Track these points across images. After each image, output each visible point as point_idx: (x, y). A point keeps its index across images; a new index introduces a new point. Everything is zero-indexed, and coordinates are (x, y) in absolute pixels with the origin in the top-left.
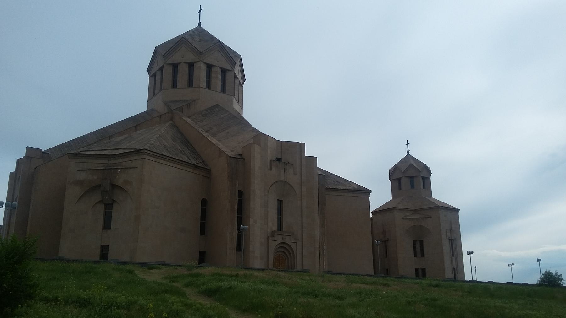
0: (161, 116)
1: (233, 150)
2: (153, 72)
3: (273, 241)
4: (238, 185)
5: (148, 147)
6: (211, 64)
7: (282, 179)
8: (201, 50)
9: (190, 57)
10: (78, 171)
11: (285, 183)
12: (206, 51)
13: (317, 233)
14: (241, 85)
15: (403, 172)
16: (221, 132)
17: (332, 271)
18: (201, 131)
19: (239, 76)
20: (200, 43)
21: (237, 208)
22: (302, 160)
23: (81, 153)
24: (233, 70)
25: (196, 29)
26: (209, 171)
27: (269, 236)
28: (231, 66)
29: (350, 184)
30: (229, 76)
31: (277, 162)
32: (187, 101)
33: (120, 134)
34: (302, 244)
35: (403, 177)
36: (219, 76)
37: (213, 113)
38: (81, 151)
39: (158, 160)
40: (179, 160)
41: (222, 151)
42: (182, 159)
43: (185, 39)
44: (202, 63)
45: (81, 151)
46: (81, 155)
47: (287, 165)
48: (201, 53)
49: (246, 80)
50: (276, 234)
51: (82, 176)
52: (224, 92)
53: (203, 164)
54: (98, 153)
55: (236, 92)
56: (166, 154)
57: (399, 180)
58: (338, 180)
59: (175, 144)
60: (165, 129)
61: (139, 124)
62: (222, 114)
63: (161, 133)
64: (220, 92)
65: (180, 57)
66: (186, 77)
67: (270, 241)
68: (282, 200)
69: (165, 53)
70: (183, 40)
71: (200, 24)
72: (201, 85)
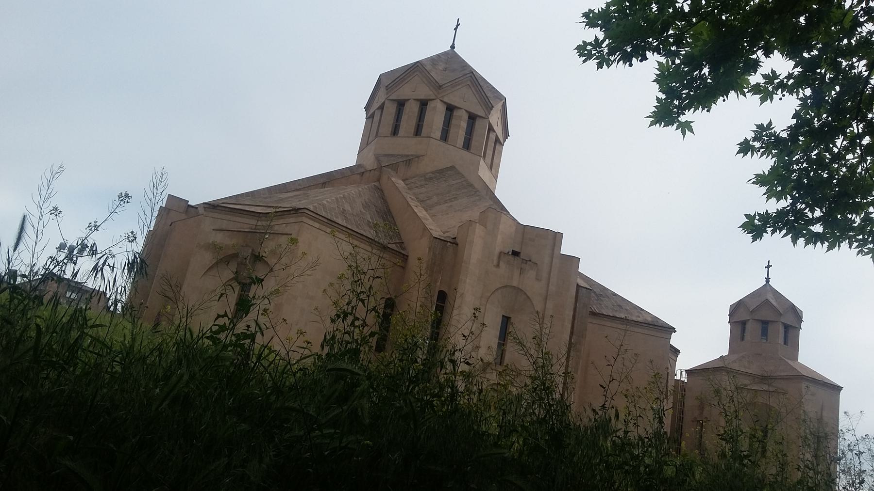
0: (363, 173)
1: (449, 230)
2: (372, 111)
4: (439, 283)
5: (313, 206)
6: (453, 104)
7: (515, 284)
8: (441, 83)
9: (424, 92)
10: (213, 230)
11: (518, 290)
12: (449, 84)
14: (498, 143)
15: (751, 312)
16: (440, 205)
18: (410, 199)
19: (499, 130)
20: (444, 72)
22: (554, 259)
23: (222, 205)
24: (486, 117)
25: (445, 54)
26: (405, 258)
28: (486, 111)
29: (641, 313)
30: (480, 127)
31: (511, 258)
32: (408, 156)
33: (297, 190)
35: (750, 321)
36: (464, 125)
37: (441, 178)
38: (223, 203)
39: (324, 228)
40: (359, 233)
41: (426, 227)
42: (362, 232)
43: (421, 65)
44: (439, 101)
45: (223, 203)
46: (220, 208)
47: (526, 264)
48: (440, 86)
49: (509, 136)
51: (219, 238)
52: (468, 149)
53: (399, 246)
54: (247, 208)
55: (490, 152)
56: (340, 221)
57: (744, 323)
58: (622, 303)
59: (364, 212)
60: (358, 190)
61: (329, 182)
62: (454, 180)
63: (348, 194)
64: (462, 149)
65: (413, 91)
66: (414, 122)
68: (510, 318)
69: (390, 84)
70: (418, 66)
71: (453, 47)
72: (433, 135)
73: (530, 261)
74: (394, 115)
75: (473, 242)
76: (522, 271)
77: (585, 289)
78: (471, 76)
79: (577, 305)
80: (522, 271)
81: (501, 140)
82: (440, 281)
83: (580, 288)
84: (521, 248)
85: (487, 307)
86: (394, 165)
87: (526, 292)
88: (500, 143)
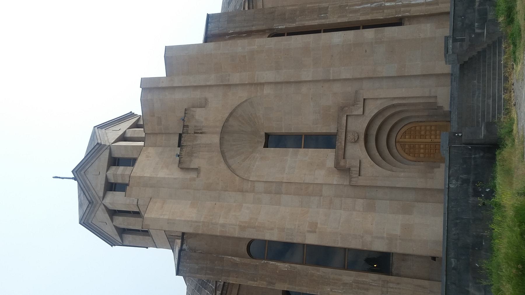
3: (362, 173)
4: (235, 258)
7: (216, 139)
9: (102, 216)
11: (225, 131)
12: (87, 194)
13: (337, 37)
17: (447, 38)
21: (287, 265)
24: (109, 148)
27: (348, 183)
34: (365, 78)
44: (103, 202)
47: (187, 126)
48: (90, 203)
49: (131, 112)
50: (342, 163)
67: (361, 181)
72: (135, 203)
73: (183, 120)
74: (134, 236)
75: (168, 219)
76: (199, 132)
77: (209, 25)
78: (76, 172)
79: (231, 32)
80: (199, 132)
81: (136, 119)
82: (233, 258)
83: (209, 33)
84: (175, 133)
85: (255, 179)
86: (170, 240)
87: (224, 119)
88: (138, 120)
